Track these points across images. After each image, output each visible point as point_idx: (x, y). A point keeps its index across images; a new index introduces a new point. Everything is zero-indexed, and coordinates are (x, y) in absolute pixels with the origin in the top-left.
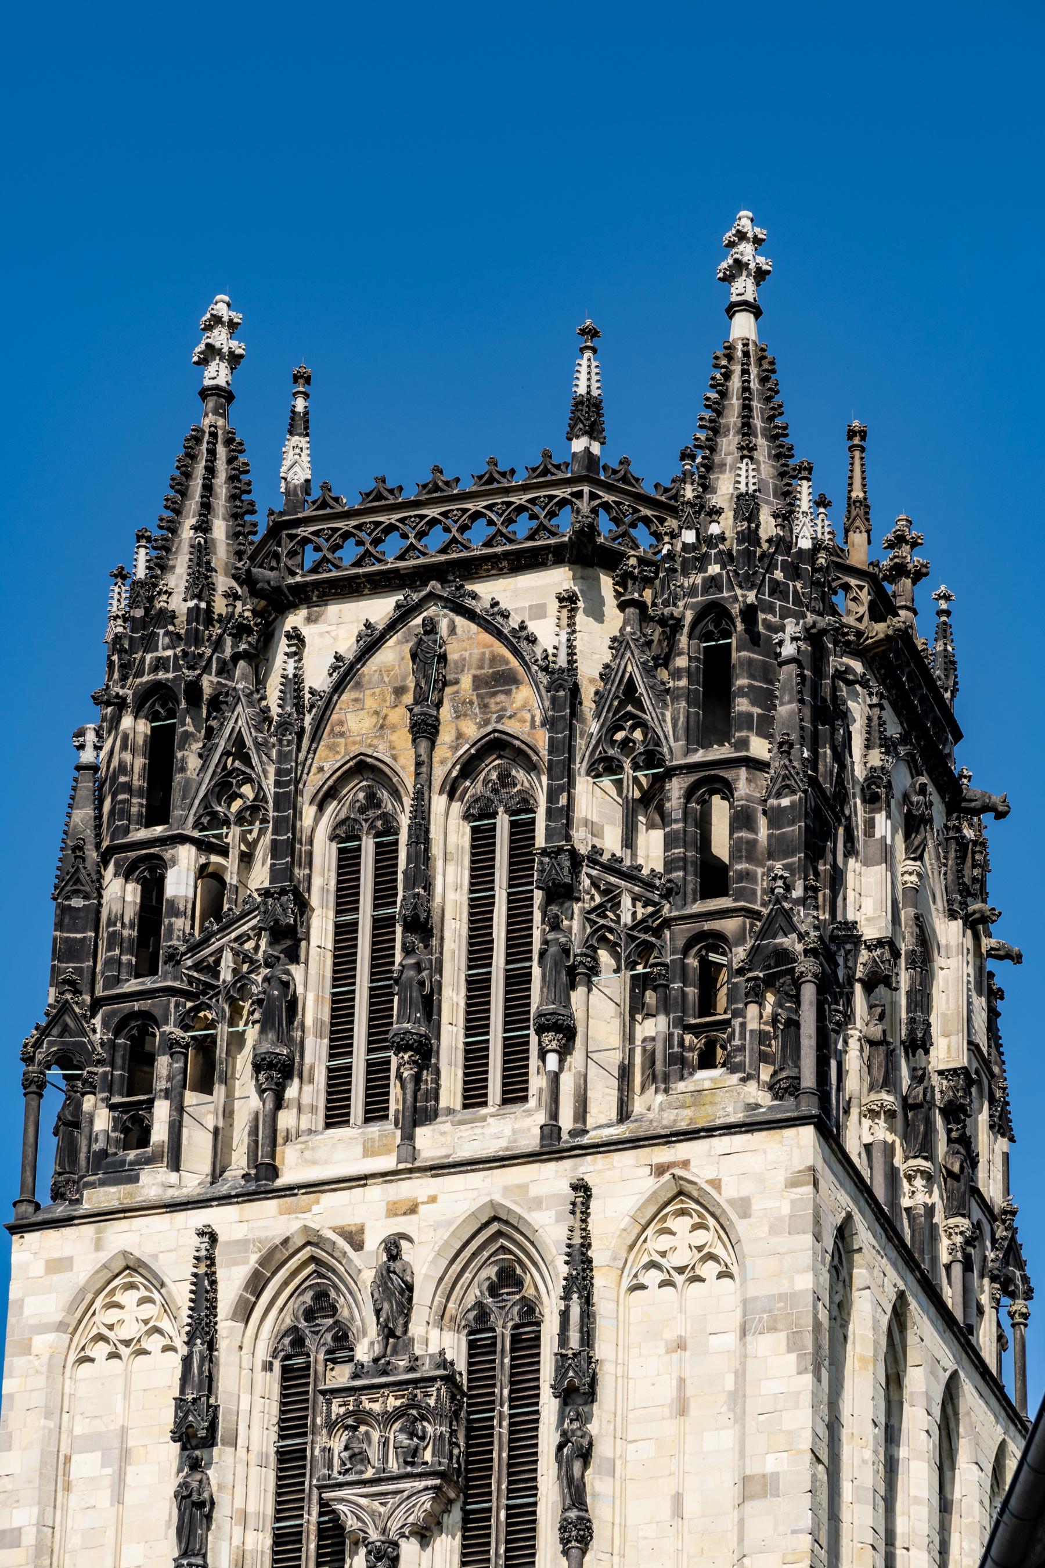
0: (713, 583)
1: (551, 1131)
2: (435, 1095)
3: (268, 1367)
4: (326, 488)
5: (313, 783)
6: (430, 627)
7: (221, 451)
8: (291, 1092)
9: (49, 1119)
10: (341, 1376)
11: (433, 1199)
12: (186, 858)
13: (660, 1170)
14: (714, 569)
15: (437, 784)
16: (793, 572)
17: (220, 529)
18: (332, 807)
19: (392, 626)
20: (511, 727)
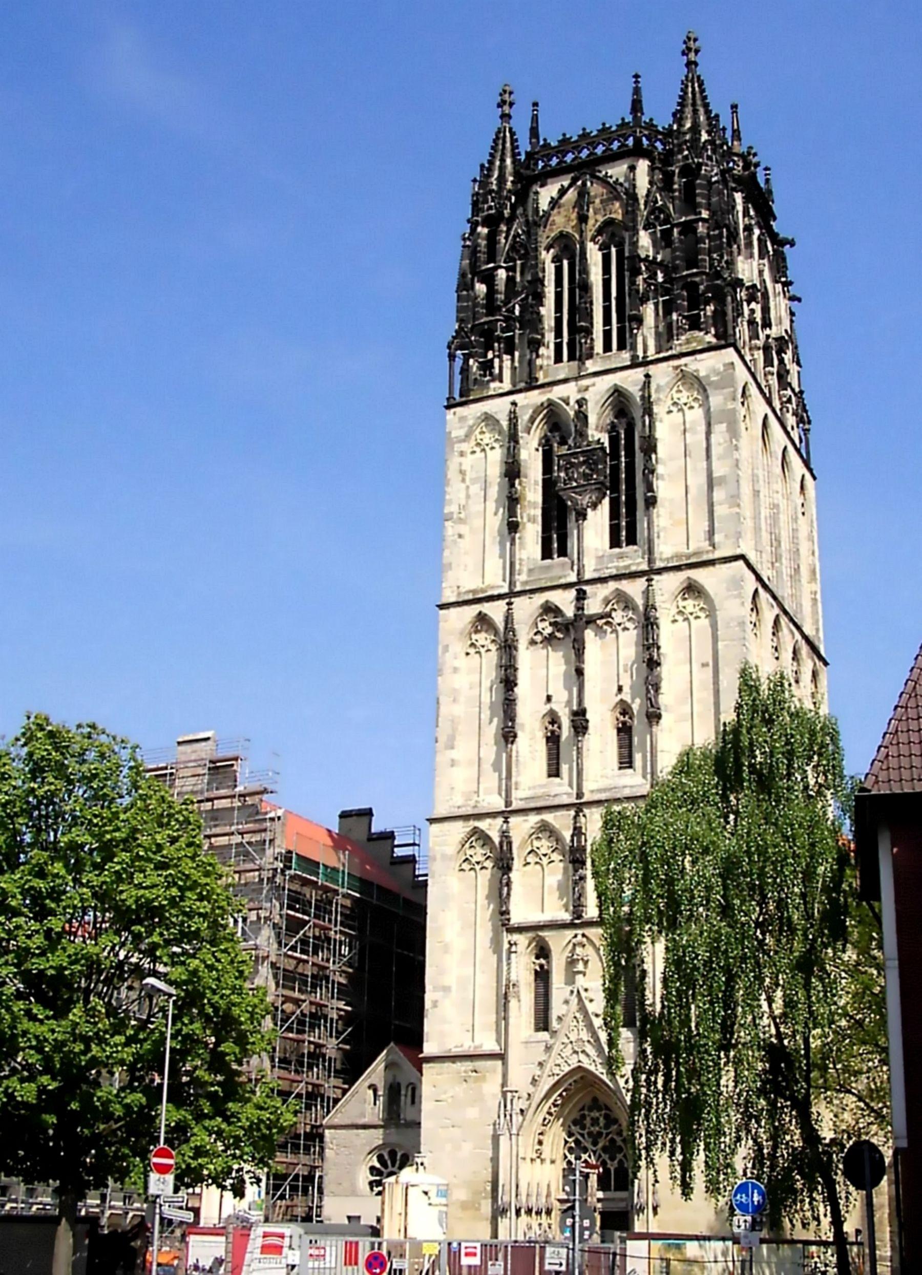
0: (686, 157)
1: (634, 357)
2: (592, 348)
3: (537, 450)
4: (545, 140)
5: (544, 242)
6: (584, 184)
7: (508, 134)
8: (542, 351)
9: (457, 370)
10: (564, 450)
11: (594, 385)
12: (502, 274)
13: (676, 368)
14: (686, 153)
15: (589, 238)
16: (714, 151)
17: (509, 161)
18: (552, 251)
19: (570, 186)
20: (613, 216)
